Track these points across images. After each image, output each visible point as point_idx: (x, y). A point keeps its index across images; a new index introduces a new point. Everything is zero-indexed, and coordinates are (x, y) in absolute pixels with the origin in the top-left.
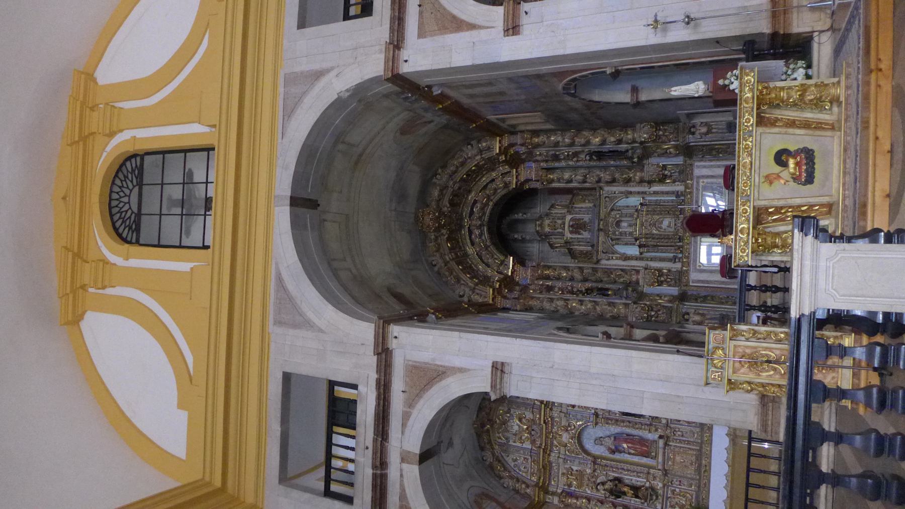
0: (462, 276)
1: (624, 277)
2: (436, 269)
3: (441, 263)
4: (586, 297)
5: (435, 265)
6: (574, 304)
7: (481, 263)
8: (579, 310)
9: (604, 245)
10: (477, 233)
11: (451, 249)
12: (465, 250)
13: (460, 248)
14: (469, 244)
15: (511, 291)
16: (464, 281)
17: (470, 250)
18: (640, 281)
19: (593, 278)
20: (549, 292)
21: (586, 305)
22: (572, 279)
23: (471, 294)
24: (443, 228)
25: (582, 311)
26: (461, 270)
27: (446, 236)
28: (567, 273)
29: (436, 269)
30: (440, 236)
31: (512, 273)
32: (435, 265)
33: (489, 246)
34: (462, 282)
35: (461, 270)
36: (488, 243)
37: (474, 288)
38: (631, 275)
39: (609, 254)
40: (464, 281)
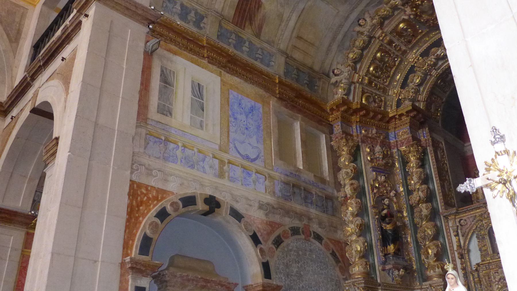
0: (366, 61)
1: (427, 258)
2: (358, 29)
3: (366, 30)
4: (373, 218)
5: (360, 25)
6: (350, 209)
7: (404, 75)
8: (346, 216)
9: (471, 219)
10: (439, 53)
11: (400, 34)
12: (412, 49)
13: (410, 42)
14: (421, 50)
15: (363, 124)
16: (360, 68)
17: (412, 56)
18: (428, 283)
19: (417, 220)
20: (373, 171)
21: (352, 222)
22: (409, 192)
23: (343, 81)
24: (412, 8)
25: (346, 219)
26: (375, 57)
27: (406, 17)
28: (415, 184)
29: (358, 29)
30: (402, 10)
31: (394, 117)
32: (360, 25)
33: (431, 75)
34: (358, 66)
35: (375, 57)
36: (434, 72)
37: (354, 83)
38: (433, 268)
39: (461, 229)
40: (360, 68)
